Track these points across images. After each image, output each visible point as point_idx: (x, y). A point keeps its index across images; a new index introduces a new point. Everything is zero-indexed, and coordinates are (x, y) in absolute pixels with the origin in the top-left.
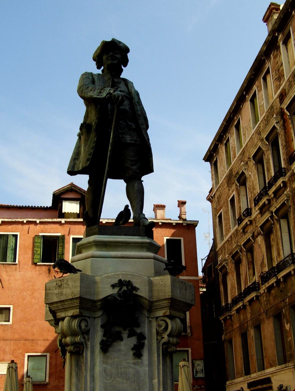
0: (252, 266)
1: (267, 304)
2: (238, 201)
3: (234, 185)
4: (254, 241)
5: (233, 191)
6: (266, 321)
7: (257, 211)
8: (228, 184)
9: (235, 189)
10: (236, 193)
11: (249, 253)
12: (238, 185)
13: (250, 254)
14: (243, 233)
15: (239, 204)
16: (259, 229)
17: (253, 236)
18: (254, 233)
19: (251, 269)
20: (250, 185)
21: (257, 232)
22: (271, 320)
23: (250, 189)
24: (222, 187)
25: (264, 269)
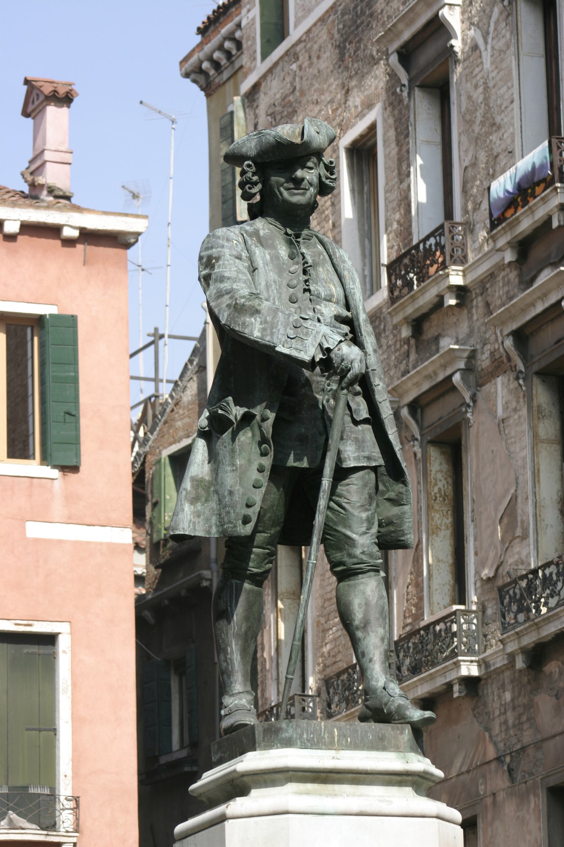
0: (449, 520)
1: (519, 725)
2: (394, 165)
3: (380, 70)
4: (474, 398)
5: (369, 106)
6: (510, 809)
7: (499, 250)
8: (342, 58)
9: (383, 96)
10: (385, 120)
11: (434, 453)
12: (405, 81)
13: (443, 453)
14: (413, 342)
15: (401, 182)
16: (509, 343)
17: (469, 370)
18: (472, 356)
19: (442, 533)
20: (469, 97)
21: (492, 354)
22: (538, 803)
23: (468, 117)
24: (303, 58)
25: (517, 549)
